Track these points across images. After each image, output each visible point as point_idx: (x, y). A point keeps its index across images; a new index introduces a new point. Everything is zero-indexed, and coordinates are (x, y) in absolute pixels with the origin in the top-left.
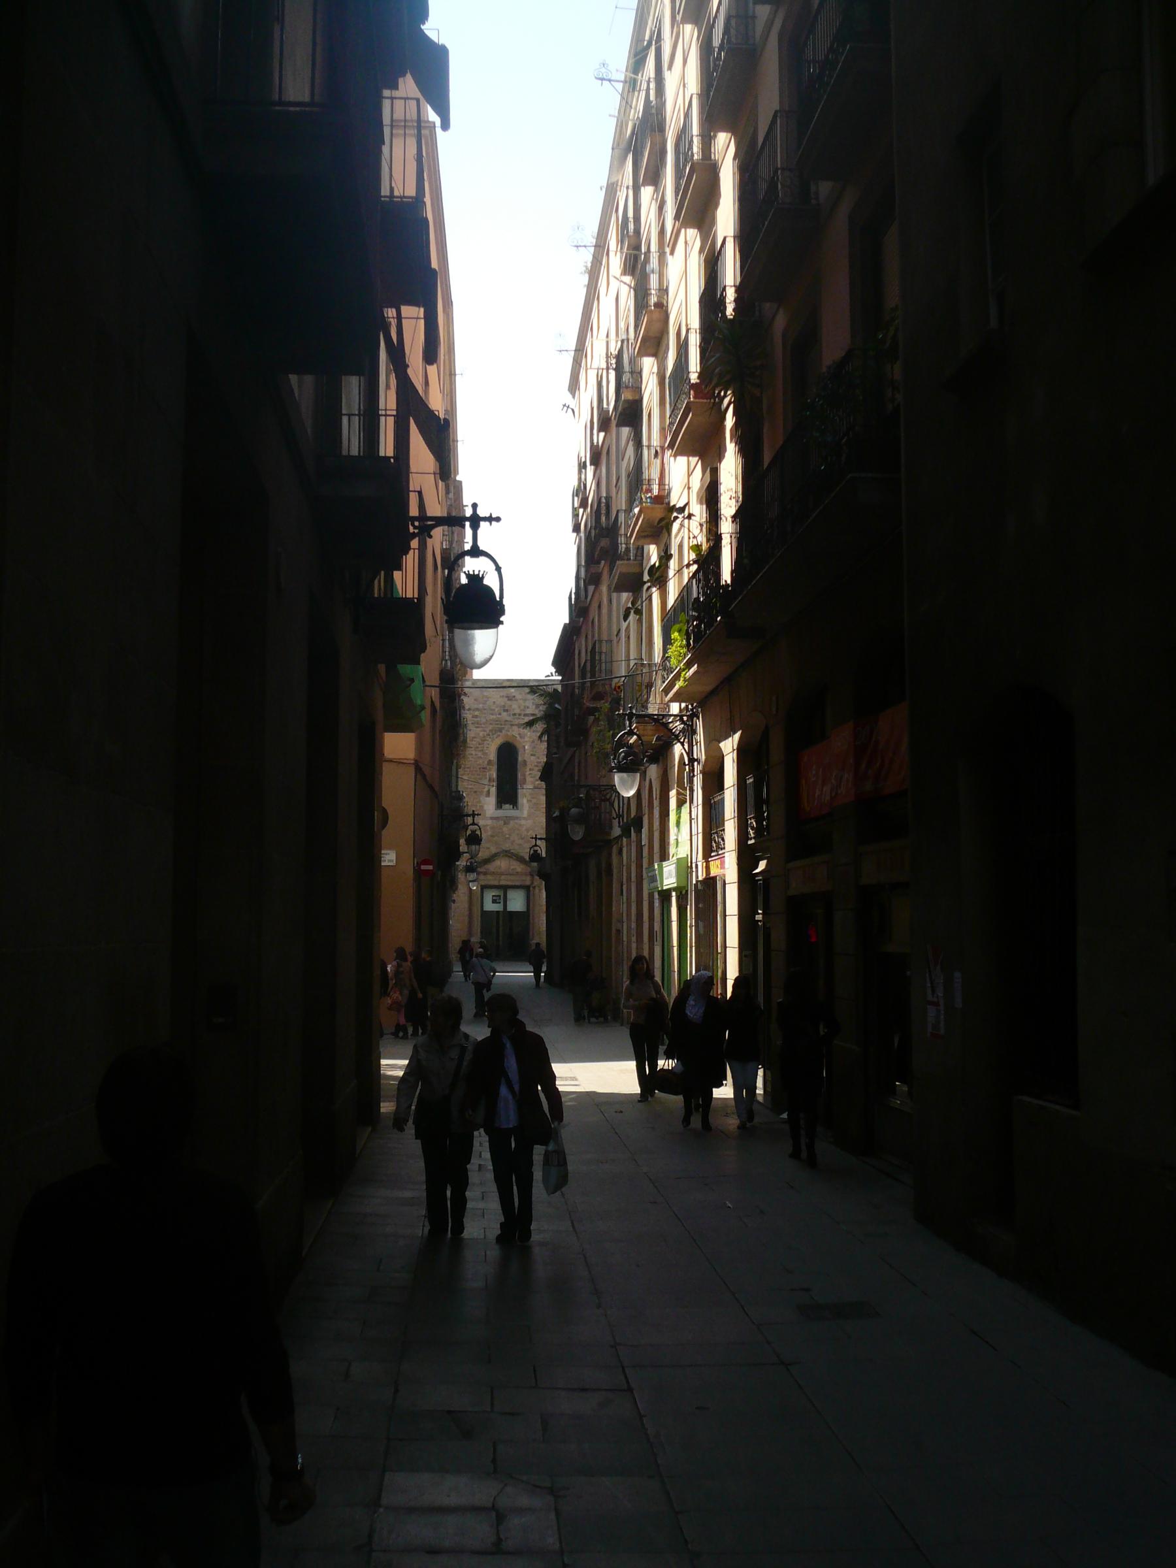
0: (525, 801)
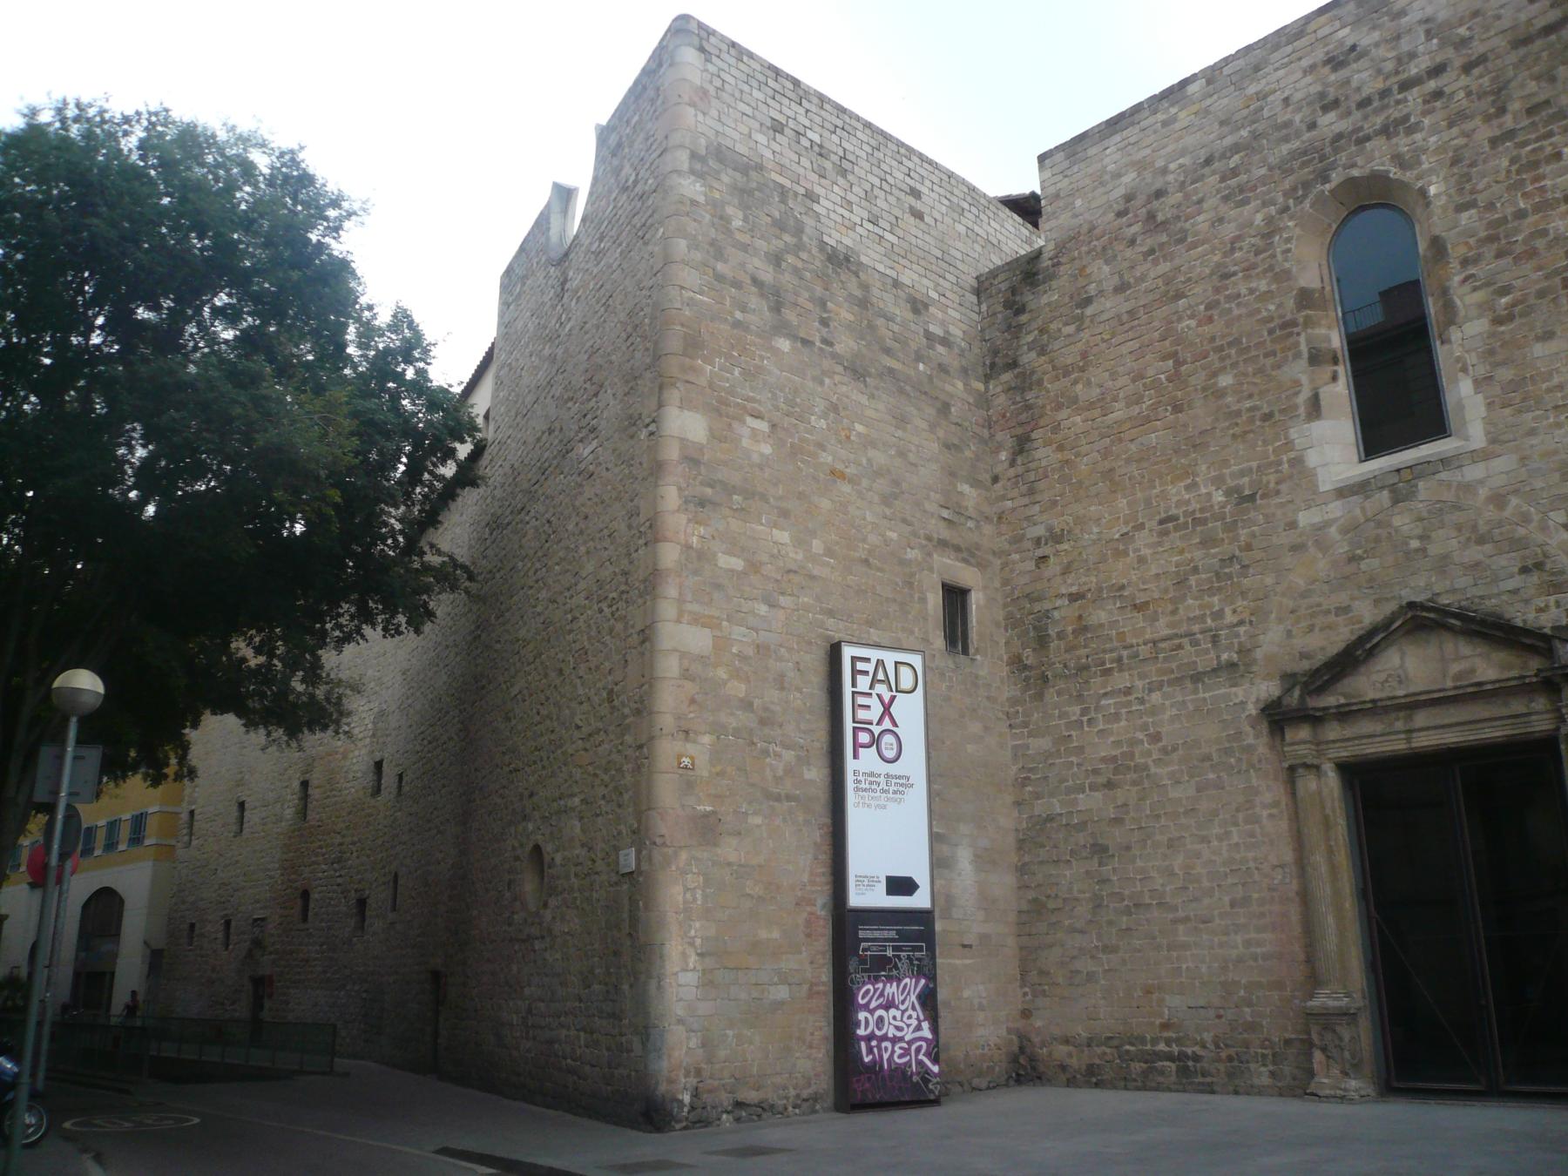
0: (1465, 387)
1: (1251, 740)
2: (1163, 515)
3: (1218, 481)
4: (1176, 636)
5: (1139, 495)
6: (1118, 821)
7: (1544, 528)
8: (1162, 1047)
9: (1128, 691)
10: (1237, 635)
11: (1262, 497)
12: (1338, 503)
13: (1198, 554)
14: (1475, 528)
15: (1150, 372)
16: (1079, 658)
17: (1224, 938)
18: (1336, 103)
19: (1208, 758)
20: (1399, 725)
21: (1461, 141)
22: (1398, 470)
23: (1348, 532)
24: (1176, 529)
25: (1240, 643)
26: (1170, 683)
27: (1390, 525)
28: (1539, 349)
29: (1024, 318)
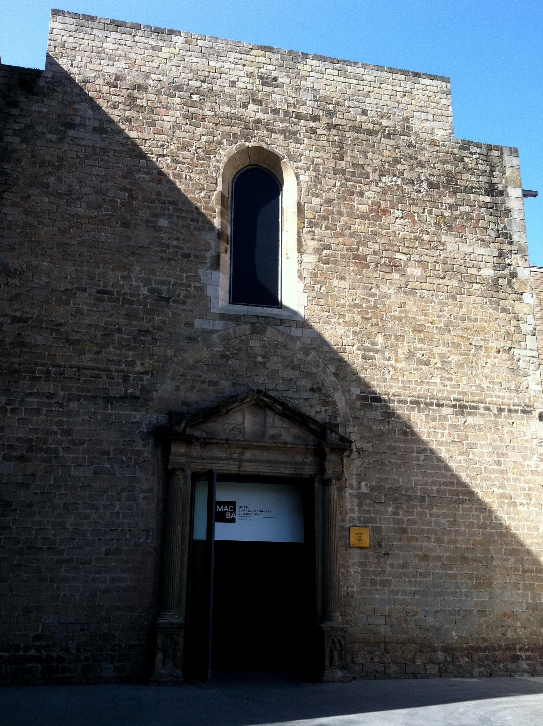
1: (140, 448)
2: (101, 288)
3: (146, 281)
4: (97, 368)
5: (85, 268)
6: (25, 485)
7: (325, 372)
8: (33, 652)
9: (51, 396)
10: (142, 380)
11: (174, 302)
12: (221, 322)
13: (123, 321)
14: (292, 361)
15: (110, 194)
16: (12, 363)
17: (96, 576)
18: (259, 102)
19: (108, 453)
20: (235, 456)
21: (319, 161)
22: (258, 316)
23: (223, 341)
24: (110, 300)
25: (143, 385)
26: (86, 398)
27: (247, 344)
28: (335, 282)
29: (15, 111)
